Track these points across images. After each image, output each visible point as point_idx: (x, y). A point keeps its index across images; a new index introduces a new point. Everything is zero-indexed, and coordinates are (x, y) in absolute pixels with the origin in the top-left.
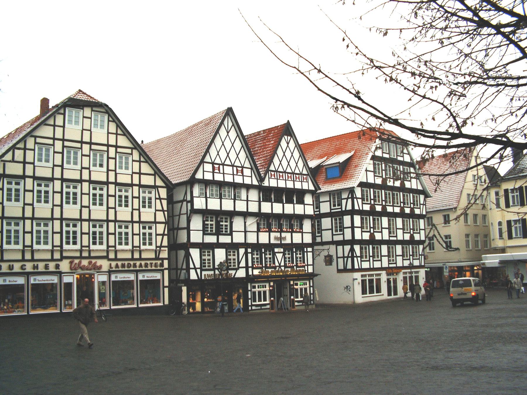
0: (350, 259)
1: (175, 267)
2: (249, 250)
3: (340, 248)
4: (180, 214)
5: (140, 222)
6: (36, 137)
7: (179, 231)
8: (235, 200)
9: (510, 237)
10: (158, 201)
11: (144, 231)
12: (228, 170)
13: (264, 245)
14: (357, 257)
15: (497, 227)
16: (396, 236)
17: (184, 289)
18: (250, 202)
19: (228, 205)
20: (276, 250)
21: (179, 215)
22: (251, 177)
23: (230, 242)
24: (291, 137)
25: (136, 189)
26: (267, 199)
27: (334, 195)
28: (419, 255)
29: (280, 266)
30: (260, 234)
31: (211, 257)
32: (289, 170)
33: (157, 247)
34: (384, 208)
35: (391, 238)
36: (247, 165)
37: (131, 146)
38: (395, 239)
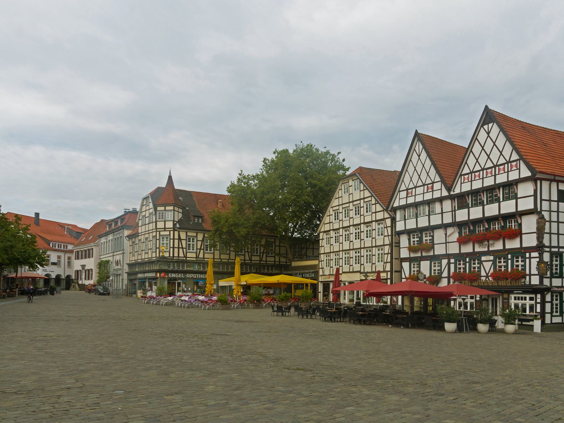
2: (452, 261)
6: (332, 207)
8: (429, 215)
10: (386, 229)
13: (468, 254)
18: (445, 213)
19: (423, 222)
20: (483, 258)
22: (441, 189)
26: (463, 205)
33: (384, 263)
36: (438, 179)
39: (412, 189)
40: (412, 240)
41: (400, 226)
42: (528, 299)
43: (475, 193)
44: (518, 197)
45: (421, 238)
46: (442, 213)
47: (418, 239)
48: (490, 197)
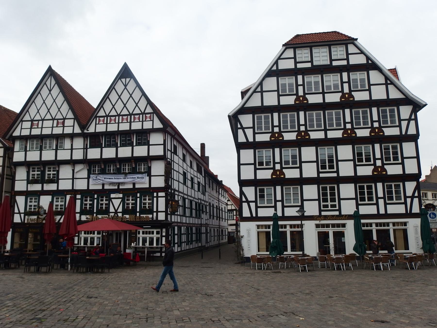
8: (56, 150)
13: (96, 191)
14: (248, 202)
19: (48, 155)
20: (112, 196)
22: (73, 126)
35: (322, 175)
36: (70, 115)
38: (335, 175)
39: (38, 121)
40: (31, 173)
41: (18, 157)
42: (155, 233)
43: (109, 135)
44: (150, 143)
45: (43, 173)
46: (72, 149)
47: (39, 173)
48: (123, 141)
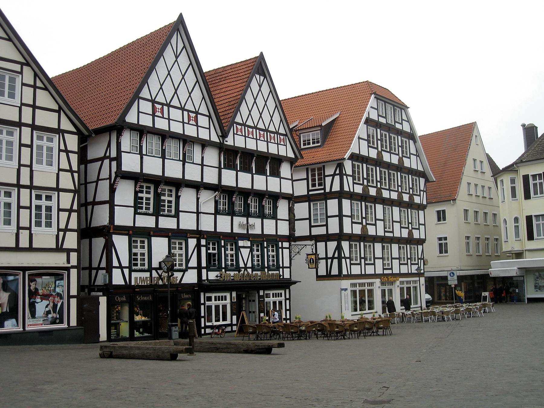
0: (336, 261)
1: (87, 265)
2: (203, 242)
3: (321, 246)
4: (98, 179)
5: (31, 187)
7: (96, 207)
8: (184, 162)
9: (530, 237)
10: (63, 155)
11: (39, 202)
12: (176, 114)
14: (345, 258)
15: (511, 225)
16: (393, 232)
17: (103, 300)
18: (205, 166)
19: (174, 170)
20: (241, 243)
21: (97, 182)
22: (209, 129)
23: (175, 227)
24: (265, 77)
25: (26, 131)
26: (230, 165)
27: (313, 170)
28: (418, 259)
29: (246, 268)
30: (218, 217)
31: (146, 251)
32: (261, 126)
34: (379, 191)
35: (387, 234)
36: (203, 110)
37: (23, 61)
